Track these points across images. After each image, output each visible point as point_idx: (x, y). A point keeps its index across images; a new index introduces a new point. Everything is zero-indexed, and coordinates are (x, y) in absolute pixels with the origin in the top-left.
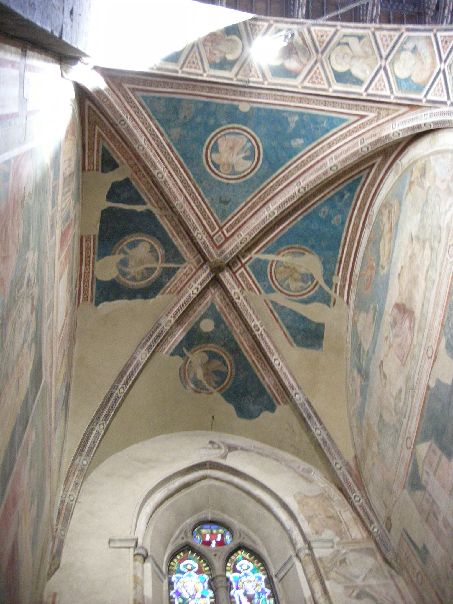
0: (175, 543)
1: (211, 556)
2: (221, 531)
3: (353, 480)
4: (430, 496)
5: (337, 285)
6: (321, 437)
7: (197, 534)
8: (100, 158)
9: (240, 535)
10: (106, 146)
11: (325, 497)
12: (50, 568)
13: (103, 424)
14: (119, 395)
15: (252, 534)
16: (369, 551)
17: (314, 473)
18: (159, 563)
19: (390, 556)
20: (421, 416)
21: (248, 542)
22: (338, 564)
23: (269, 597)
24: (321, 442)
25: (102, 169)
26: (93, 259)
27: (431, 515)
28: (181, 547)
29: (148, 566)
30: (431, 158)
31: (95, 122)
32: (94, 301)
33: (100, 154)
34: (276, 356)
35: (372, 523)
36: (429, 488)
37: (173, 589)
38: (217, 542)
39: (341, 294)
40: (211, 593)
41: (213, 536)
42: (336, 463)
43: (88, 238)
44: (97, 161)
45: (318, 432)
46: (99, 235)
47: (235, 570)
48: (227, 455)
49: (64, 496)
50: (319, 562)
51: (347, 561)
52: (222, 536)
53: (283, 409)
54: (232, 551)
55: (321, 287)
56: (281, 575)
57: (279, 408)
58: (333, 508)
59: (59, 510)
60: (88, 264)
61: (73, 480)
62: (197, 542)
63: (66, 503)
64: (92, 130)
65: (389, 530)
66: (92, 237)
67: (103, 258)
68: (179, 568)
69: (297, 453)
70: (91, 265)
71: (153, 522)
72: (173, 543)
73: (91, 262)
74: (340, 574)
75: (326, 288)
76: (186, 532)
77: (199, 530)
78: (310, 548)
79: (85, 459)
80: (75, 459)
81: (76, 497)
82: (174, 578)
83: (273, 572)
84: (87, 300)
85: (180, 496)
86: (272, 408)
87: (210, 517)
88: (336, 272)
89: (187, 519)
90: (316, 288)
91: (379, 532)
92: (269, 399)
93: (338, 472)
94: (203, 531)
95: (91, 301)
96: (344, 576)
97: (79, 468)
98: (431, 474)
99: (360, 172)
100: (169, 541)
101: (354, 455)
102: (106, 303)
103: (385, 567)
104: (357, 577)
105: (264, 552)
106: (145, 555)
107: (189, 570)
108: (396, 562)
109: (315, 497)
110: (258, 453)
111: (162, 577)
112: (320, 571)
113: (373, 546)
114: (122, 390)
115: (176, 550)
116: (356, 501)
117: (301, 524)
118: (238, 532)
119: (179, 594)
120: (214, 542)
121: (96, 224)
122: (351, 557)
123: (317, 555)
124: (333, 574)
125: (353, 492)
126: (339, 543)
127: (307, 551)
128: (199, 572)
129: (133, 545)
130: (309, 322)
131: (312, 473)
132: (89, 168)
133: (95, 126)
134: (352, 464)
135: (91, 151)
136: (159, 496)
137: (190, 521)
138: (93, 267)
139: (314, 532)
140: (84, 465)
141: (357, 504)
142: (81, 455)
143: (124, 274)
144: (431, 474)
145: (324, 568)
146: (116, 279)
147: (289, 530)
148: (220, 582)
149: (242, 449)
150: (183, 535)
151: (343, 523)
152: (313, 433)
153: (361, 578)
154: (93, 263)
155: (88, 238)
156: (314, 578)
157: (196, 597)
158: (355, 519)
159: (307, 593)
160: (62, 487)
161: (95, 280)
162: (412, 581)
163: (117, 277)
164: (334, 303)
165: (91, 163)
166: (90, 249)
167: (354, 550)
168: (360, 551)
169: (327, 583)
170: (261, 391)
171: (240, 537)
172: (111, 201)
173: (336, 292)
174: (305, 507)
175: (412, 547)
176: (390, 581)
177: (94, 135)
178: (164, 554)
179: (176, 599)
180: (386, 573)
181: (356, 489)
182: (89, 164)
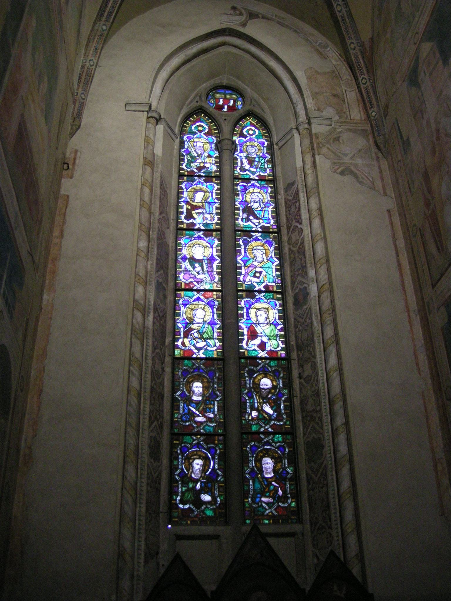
2: (234, 96)
3: (364, 62)
4: (422, 95)
6: (341, 14)
7: (211, 99)
9: (251, 102)
11: (335, 75)
12: (72, 129)
15: (262, 103)
16: (363, 133)
17: (331, 48)
18: (171, 124)
19: (380, 140)
20: (432, 15)
21: (257, 110)
22: (331, 141)
23: (268, 162)
24: (340, 19)
29: (160, 127)
37: (184, 147)
38: (229, 107)
40: (216, 154)
41: (226, 101)
42: (351, 43)
45: (339, 8)
47: (242, 135)
48: (247, 22)
49: (84, 61)
50: (314, 138)
51: (340, 139)
52: (235, 102)
54: (241, 117)
56: (280, 144)
58: (340, 87)
59: (80, 74)
61: (93, 45)
63: (86, 68)
65: (385, 117)
68: (191, 129)
69: (318, 26)
71: (169, 86)
72: (188, 106)
74: (331, 151)
76: (200, 97)
77: (213, 95)
78: (309, 123)
80: (95, 24)
81: (95, 62)
82: (185, 138)
83: (275, 140)
87: (225, 82)
89: (203, 84)
91: (376, 117)
93: (351, 52)
94: (218, 96)
96: (334, 153)
97: (99, 33)
98: (427, 75)
100: (183, 105)
101: (371, 37)
103: (374, 150)
104: (346, 155)
105: (270, 120)
107: (200, 132)
108: (385, 147)
109: (325, 73)
110: (279, 23)
111: (173, 136)
112: (313, 146)
113: (369, 128)
116: (363, 84)
117: (306, 100)
118: (249, 99)
119: (188, 152)
120: (226, 107)
122: (346, 136)
123: (314, 131)
124: (324, 150)
125: (362, 73)
126: (337, 122)
127: (306, 126)
128: (208, 134)
129: (147, 109)
131: (328, 49)
134: (367, 45)
136: (176, 61)
137: (206, 86)
139: (316, 109)
140: (103, 30)
141: (362, 86)
142: (100, 20)
145: (318, 143)
147: (295, 103)
148: (226, 145)
149: (264, 17)
150: (197, 99)
151: (346, 103)
152: (334, 9)
153: (350, 156)
156: (307, 150)
157: (203, 156)
158: (358, 100)
159: (299, 163)
160: (83, 52)
162: (393, 166)
167: (350, 130)
168: (354, 131)
169: (317, 157)
171: (250, 105)
174: (313, 83)
175: (399, 137)
176: (375, 163)
178: (178, 115)
179: (185, 158)
180: (374, 155)
181: (365, 72)
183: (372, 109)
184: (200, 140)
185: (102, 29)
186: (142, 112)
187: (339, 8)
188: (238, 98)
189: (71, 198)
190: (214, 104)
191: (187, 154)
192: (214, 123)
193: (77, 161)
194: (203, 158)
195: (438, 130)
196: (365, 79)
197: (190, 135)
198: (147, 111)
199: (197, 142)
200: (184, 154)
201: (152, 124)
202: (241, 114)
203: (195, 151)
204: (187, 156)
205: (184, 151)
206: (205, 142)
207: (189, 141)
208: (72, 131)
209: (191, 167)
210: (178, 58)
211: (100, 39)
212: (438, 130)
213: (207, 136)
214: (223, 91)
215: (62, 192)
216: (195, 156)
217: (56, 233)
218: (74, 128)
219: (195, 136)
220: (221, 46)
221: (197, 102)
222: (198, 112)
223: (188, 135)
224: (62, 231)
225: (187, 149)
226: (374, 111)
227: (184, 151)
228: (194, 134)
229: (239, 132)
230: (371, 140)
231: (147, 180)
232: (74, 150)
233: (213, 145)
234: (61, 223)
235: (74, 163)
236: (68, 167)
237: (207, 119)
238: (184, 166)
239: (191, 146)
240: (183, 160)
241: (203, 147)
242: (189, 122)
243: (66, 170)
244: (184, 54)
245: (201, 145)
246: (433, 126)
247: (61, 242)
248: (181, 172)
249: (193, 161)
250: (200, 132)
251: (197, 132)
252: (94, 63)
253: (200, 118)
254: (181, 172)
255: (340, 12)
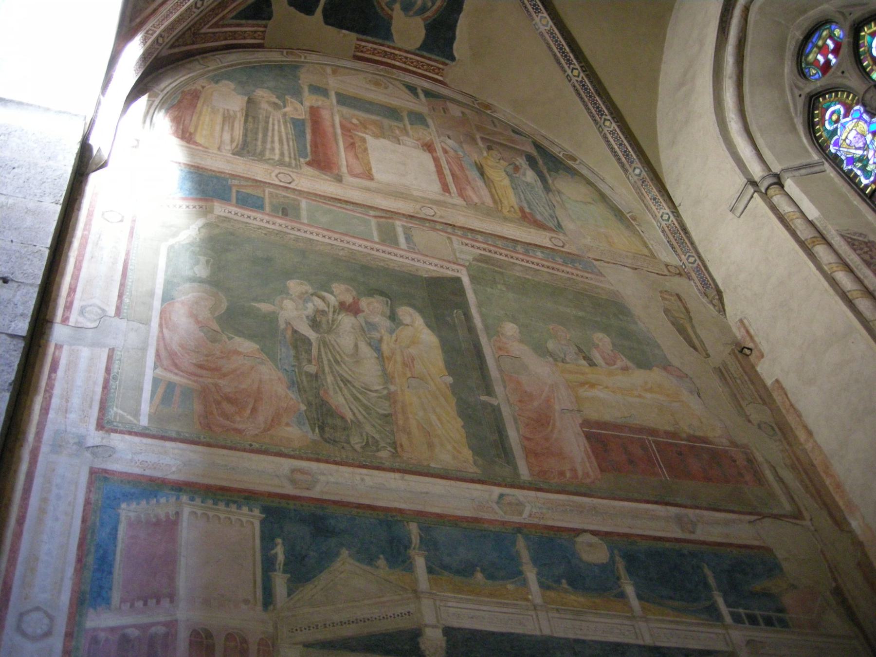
0: (799, 112)
1: (840, 81)
2: (825, 33)
7: (809, 71)
8: (250, 22)
10: (234, 13)
12: (714, 306)
13: (605, 120)
14: (580, 79)
25: (264, 19)
26: (389, 47)
28: (807, 108)
30: (144, 421)
31: (194, 34)
32: (447, 61)
33: (243, 22)
37: (842, 161)
41: (823, 50)
43: (358, 48)
44: (253, 26)
46: (357, 32)
49: (659, 224)
52: (831, 37)
59: (668, 242)
60: (394, 57)
62: (817, 80)
63: (666, 229)
64: (206, 37)
66: (359, 43)
67: (392, 34)
68: (828, 131)
70: (397, 52)
72: (796, 114)
73: (393, 51)
77: (808, 64)
79: (635, 169)
82: (833, 149)
84: (443, 70)
85: (748, 64)
87: (799, 36)
89: (783, 70)
94: (811, 57)
95: (446, 64)
100: (791, 119)
102: (455, 46)
106: (775, 180)
107: (837, 121)
114: (576, 72)
115: (806, 116)
119: (851, 160)
120: (831, 56)
121: (341, 35)
129: (751, 190)
132: (260, 37)
133: (202, 34)
135: (237, 35)
137: (788, 67)
138: (400, 50)
140: (639, 175)
143: (423, 9)
146: (427, 22)
150: (797, 92)
154: (394, 48)
155: (358, 48)
157: (868, 142)
161: (417, 52)
163: (424, 20)
165: (254, 35)
166: (375, 49)
172: (316, 9)
177: (214, 33)
178: (799, 137)
179: (855, 170)
182: (255, 38)
184: (847, 130)
185: (637, 175)
186: (753, 199)
188: (830, 28)
189: (781, 380)
190: (817, 72)
191: (852, 164)
192: (839, 91)
193: (752, 331)
194: (871, 146)
197: (834, 138)
198: (755, 191)
199: (847, 138)
200: (850, 167)
201: (776, 195)
202: (849, 42)
203: (856, 149)
204: (855, 166)
205: (848, 165)
206: (853, 124)
207: (840, 147)
208: (717, 308)
209: (871, 172)
210: (727, 91)
211: (647, 185)
213: (848, 117)
214: (810, 45)
215: (769, 382)
216: (861, 156)
217: (802, 435)
218: (716, 302)
219: (839, 133)
220: (747, 15)
221: (800, 96)
222: (814, 103)
223: (832, 142)
224: (805, 427)
225: (847, 158)
227: (848, 165)
228: (834, 131)
229: (871, 63)
231: (830, 264)
232: (739, 323)
233: (865, 116)
234: (798, 419)
235: (751, 337)
236: (748, 349)
237: (830, 97)
238: (865, 182)
239: (846, 150)
240: (856, 176)
241: (858, 133)
242: (818, 127)
243: (750, 354)
244: (727, 79)
245: (853, 133)
247: (815, 442)
248: (867, 192)
249: (865, 163)
250: (837, 121)
251: (835, 125)
252: (667, 214)
253: (822, 107)
254: (867, 192)
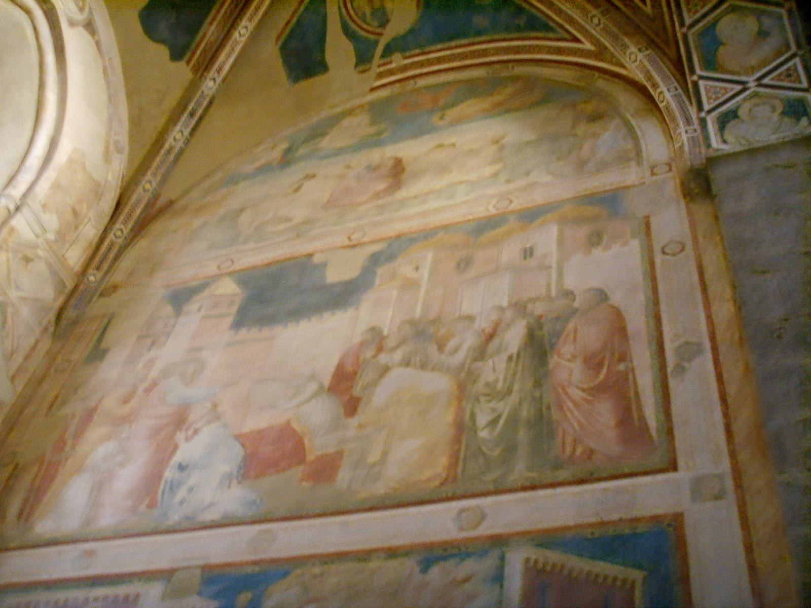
4: (174, 326)
5: (391, 62)
6: (173, 143)
11: (97, 191)
19: (70, 314)
20: (269, 265)
22: (20, 255)
24: (167, 146)
27: (149, 341)
34: (251, 27)
35: (98, 269)
36: (182, 319)
39: (380, 76)
45: (179, 136)
51: (31, 265)
53: (182, 71)
55: (376, 43)
57: (182, 64)
65: (102, 295)
69: (136, 122)
75: (379, 51)
86: (177, 55)
88: (407, 54)
90: (372, 37)
92: (186, 47)
93: (140, 190)
98: (202, 312)
99: (562, 27)
101: (173, 198)
103: (52, 316)
104: (18, 288)
113: (70, 285)
125: (125, 223)
127: (12, 207)
130: (323, 51)
141: (111, 236)
144: (202, 312)
149: (98, 44)
153: (21, 294)
158: (91, 244)
164: (364, 72)
168: (53, 272)
170: (193, 28)
173: (379, 66)
176: (38, 331)
180: (45, 321)
183: (95, 272)
187: (179, 136)
195: (155, 384)
196: (122, 232)
212: (155, 384)
226: (94, 275)
230: (61, 300)
246: (154, 373)
255: (175, 139)
